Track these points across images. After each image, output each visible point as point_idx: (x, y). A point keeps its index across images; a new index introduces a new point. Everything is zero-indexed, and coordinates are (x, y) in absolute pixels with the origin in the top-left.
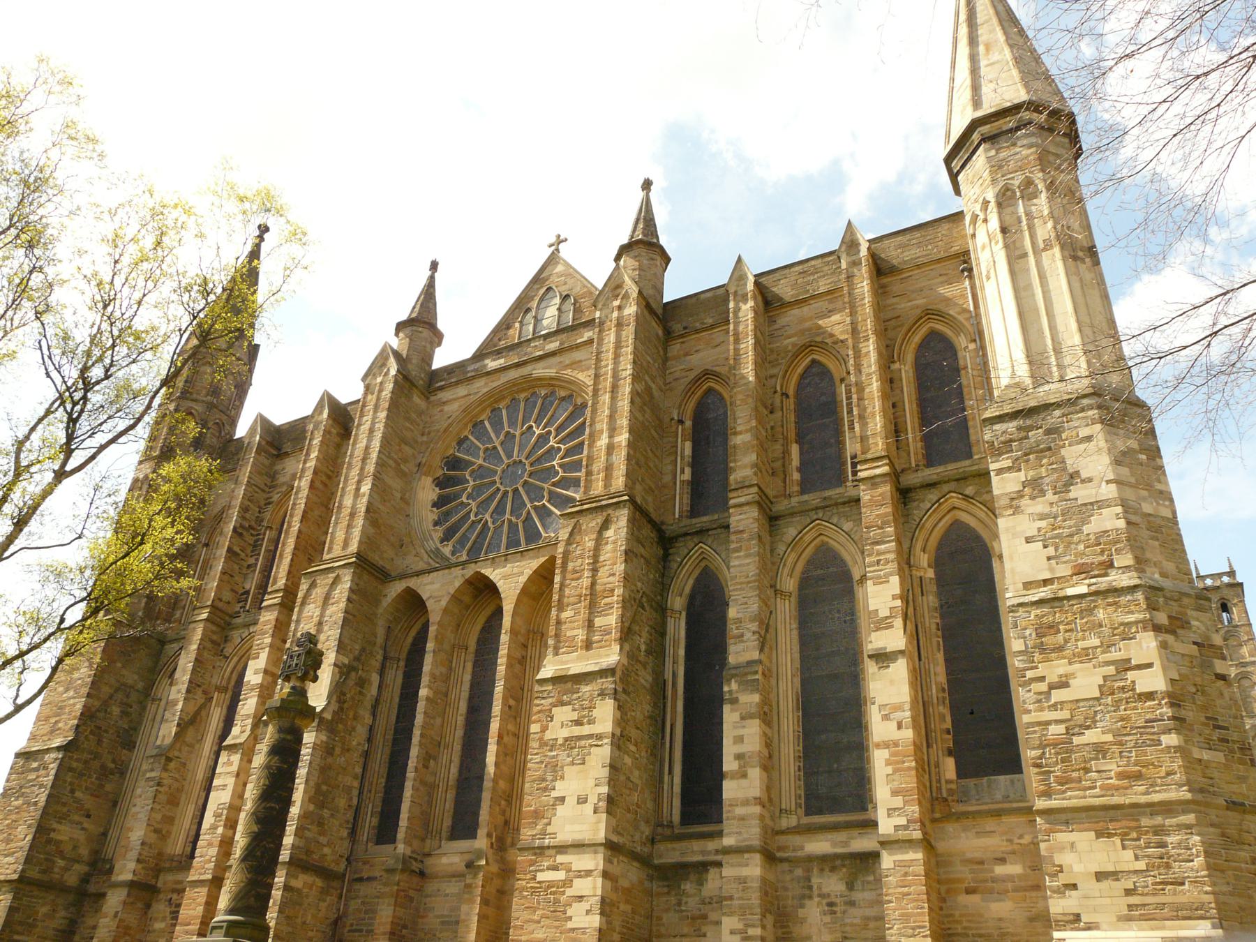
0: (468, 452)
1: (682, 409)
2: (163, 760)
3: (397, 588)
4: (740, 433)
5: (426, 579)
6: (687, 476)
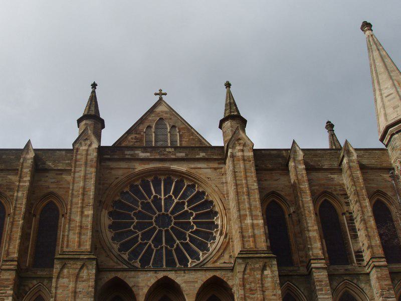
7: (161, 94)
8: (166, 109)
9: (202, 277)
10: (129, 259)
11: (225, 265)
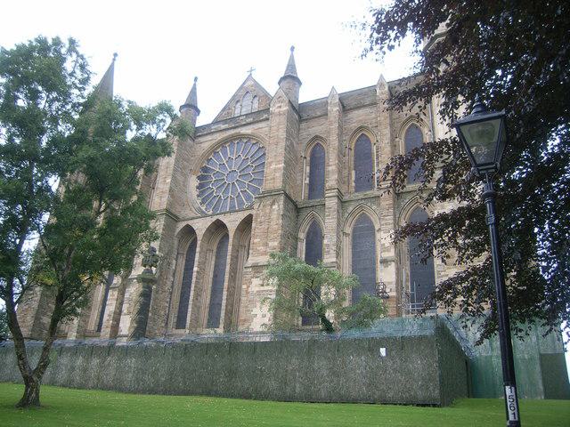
0: (212, 165)
1: (304, 152)
3: (181, 225)
5: (195, 221)
6: (307, 182)
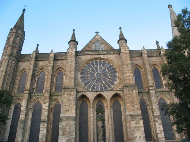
2: (23, 123)
4: (149, 77)
7: (97, 32)
8: (99, 37)
9: (113, 93)
10: (87, 88)
11: (120, 89)
